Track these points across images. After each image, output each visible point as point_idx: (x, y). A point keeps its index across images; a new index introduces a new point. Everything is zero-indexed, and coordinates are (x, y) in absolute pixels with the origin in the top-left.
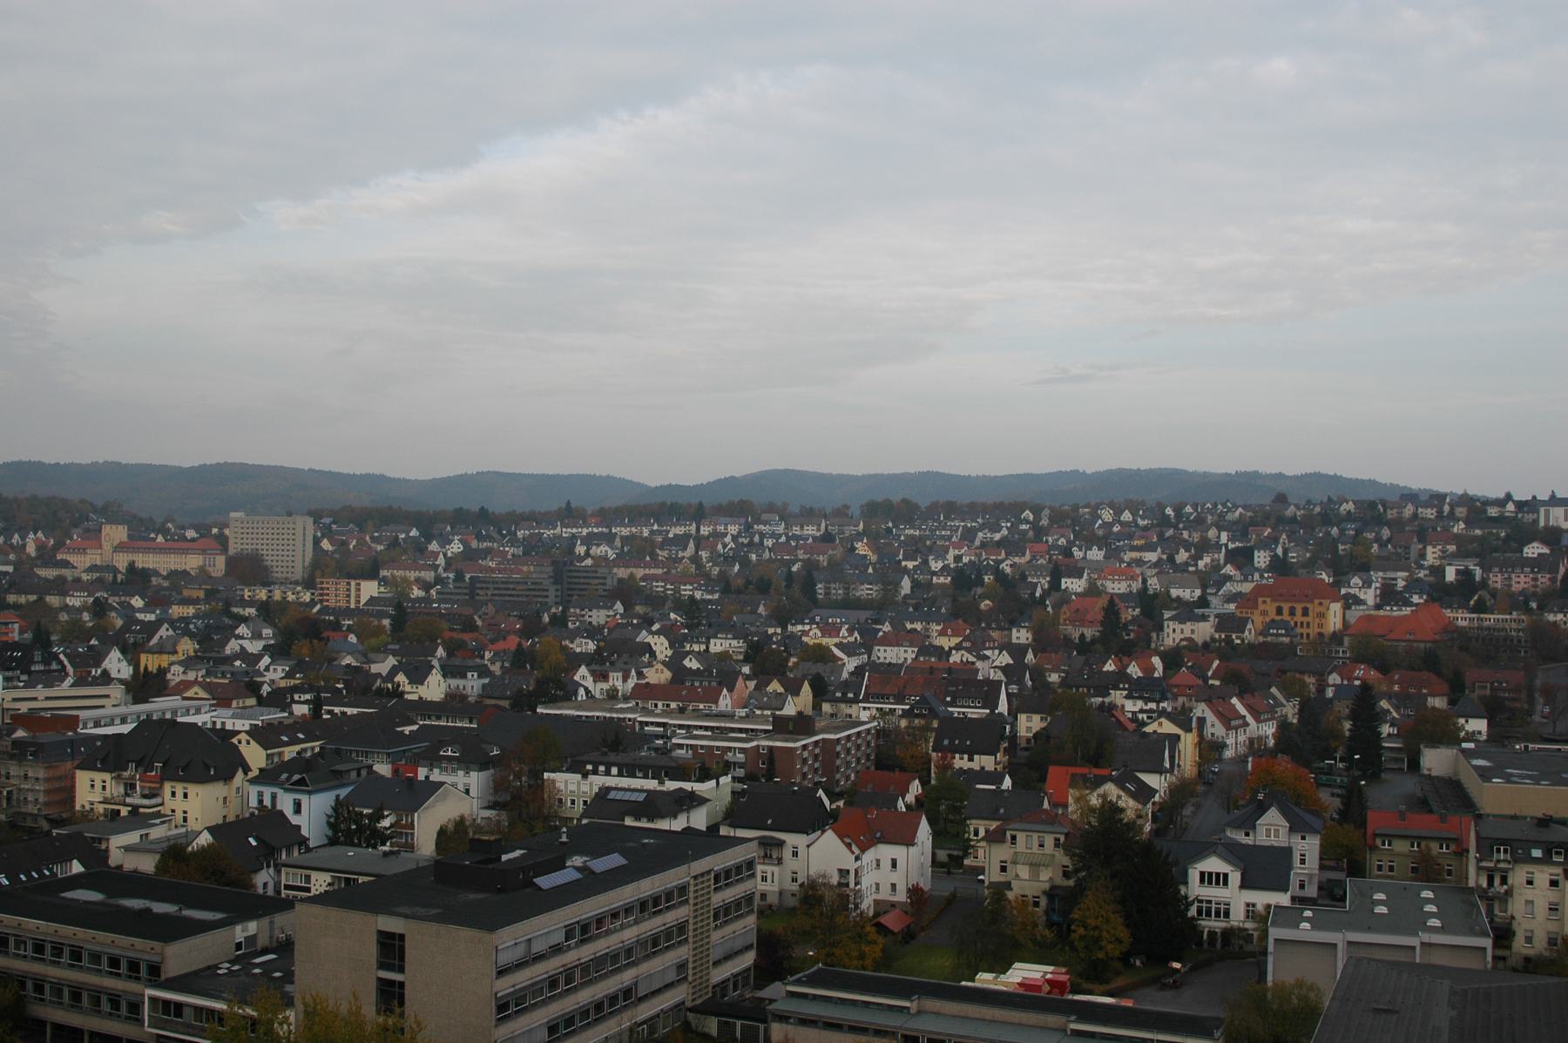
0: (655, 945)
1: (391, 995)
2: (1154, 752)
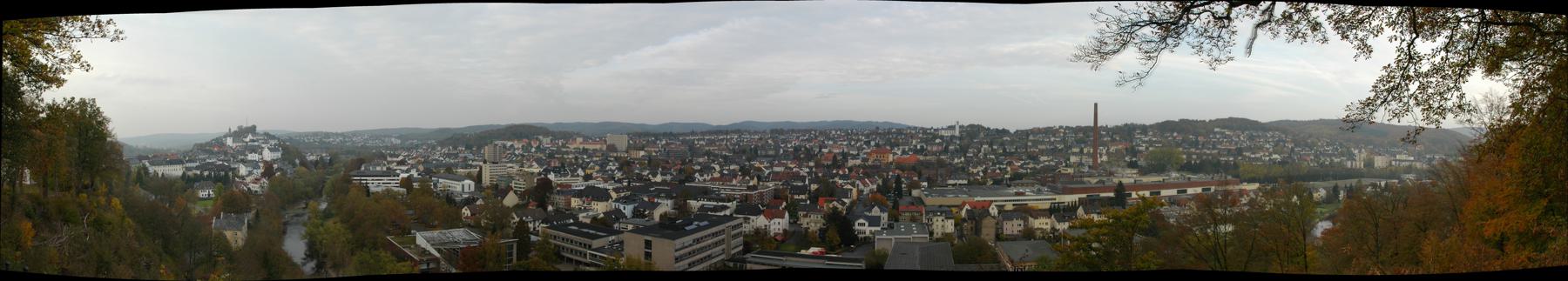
0: (716, 244)
1: (648, 255)
2: (846, 193)
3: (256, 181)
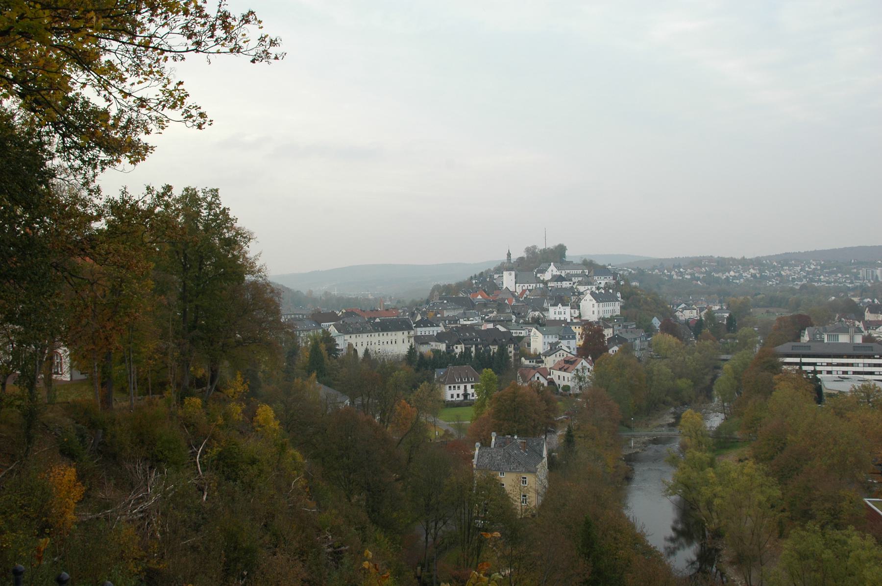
3: (567, 364)
